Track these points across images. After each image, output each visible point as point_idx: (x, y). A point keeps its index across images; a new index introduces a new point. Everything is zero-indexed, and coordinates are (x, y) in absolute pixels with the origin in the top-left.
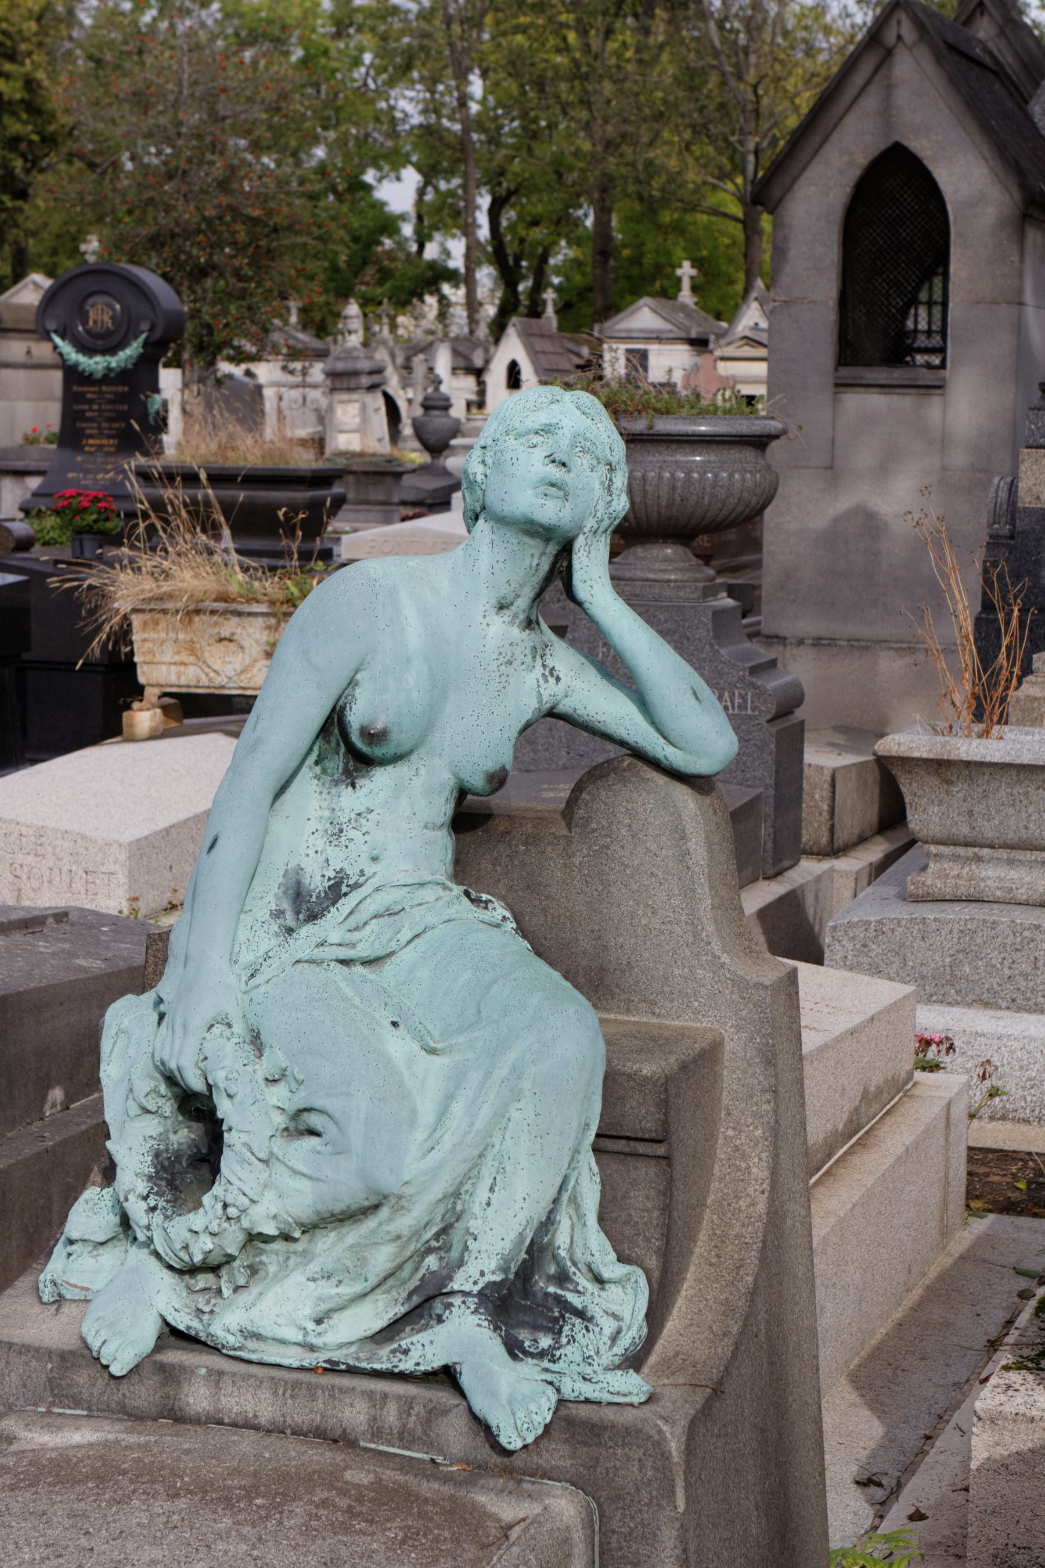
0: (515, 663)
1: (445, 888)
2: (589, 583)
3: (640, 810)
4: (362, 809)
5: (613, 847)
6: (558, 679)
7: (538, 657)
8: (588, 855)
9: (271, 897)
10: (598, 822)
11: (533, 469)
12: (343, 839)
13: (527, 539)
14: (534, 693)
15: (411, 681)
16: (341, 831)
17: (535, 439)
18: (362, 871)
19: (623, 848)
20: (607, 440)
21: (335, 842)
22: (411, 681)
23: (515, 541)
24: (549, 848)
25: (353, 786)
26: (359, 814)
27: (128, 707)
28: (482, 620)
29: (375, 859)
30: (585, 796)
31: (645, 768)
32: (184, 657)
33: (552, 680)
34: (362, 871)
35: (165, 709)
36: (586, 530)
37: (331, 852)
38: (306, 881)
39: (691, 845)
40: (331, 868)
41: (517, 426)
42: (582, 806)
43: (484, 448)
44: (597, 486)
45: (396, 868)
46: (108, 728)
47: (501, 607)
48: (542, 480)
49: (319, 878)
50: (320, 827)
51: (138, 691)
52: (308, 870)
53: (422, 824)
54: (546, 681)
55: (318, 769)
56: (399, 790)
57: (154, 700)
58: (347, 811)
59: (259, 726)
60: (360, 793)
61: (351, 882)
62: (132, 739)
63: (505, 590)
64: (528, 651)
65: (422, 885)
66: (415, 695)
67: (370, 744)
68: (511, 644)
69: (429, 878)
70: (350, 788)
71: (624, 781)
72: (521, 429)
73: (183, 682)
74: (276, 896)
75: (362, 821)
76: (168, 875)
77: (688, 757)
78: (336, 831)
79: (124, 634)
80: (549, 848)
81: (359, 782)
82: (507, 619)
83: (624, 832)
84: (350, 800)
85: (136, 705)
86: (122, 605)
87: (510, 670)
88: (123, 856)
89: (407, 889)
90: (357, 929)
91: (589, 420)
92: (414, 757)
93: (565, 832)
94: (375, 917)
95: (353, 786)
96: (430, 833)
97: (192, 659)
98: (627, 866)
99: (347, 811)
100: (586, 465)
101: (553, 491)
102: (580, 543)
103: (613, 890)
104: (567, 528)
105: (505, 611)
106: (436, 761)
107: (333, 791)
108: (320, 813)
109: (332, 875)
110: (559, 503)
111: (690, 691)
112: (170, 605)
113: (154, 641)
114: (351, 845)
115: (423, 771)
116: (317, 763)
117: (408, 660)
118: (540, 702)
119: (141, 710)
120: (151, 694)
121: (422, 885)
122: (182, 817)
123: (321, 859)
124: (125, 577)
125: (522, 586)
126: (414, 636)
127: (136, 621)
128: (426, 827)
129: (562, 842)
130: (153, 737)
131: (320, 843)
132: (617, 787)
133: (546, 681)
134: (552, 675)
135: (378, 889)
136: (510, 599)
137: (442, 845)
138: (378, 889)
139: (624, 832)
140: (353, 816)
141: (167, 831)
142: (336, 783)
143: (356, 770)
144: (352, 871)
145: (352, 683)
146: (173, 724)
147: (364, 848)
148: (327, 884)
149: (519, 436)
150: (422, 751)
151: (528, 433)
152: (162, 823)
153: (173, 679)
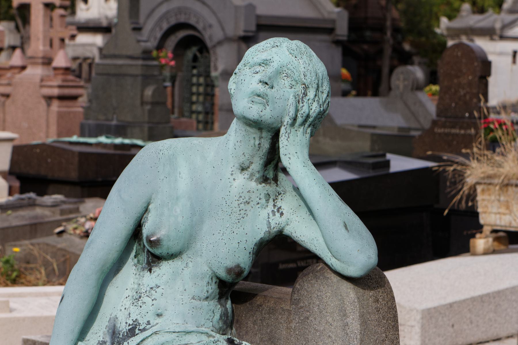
0: (252, 204)
1: (209, 336)
2: (288, 156)
3: (324, 296)
4: (153, 285)
5: (310, 319)
6: (282, 214)
7: (271, 200)
8: (299, 322)
9: (101, 334)
10: (304, 303)
11: (251, 86)
13: (248, 128)
14: (265, 222)
15: (178, 210)
16: (140, 297)
17: (258, 68)
19: (315, 319)
20: (303, 69)
21: (135, 304)
22: (178, 210)
23: (243, 129)
25: (150, 270)
26: (152, 288)
27: (473, 236)
28: (230, 176)
29: (159, 315)
32: (503, 210)
33: (278, 215)
35: (497, 239)
36: (285, 123)
37: (133, 309)
38: (118, 325)
39: (349, 320)
40: (131, 319)
41: (250, 61)
44: (291, 97)
45: (171, 322)
46: (462, 248)
47: (243, 169)
48: (252, 92)
49: (124, 324)
50: (131, 294)
51: (479, 228)
52: (120, 319)
53: (191, 297)
54: (274, 215)
55: (136, 260)
56: (175, 275)
57: (488, 233)
58: (146, 286)
60: (154, 275)
61: (141, 328)
62: (475, 254)
63: (242, 159)
64: (262, 196)
66: (180, 219)
67: (151, 247)
68: (249, 192)
69: (195, 329)
70: (149, 273)
71: (317, 278)
73: (503, 223)
74: (104, 334)
75: (153, 292)
76: (451, 329)
77: (343, 265)
78: (138, 297)
79: (472, 196)
80: (280, 317)
81: (154, 269)
82: (246, 176)
83: (316, 309)
84: (149, 279)
85: (478, 235)
86: (470, 180)
87: (248, 207)
88: (419, 317)
89: (176, 334)
91: (293, 58)
92: (184, 256)
95: (150, 270)
96: (197, 303)
97: (507, 212)
98: (317, 331)
99: (146, 286)
100: (287, 84)
101: (257, 99)
102: (282, 130)
104: (270, 121)
105: (245, 172)
106: (199, 259)
107: (141, 273)
108: (133, 286)
109: (131, 322)
110: (261, 107)
111: (342, 224)
112: (496, 181)
113: (489, 201)
114: (144, 306)
115: (190, 265)
116: (135, 257)
117: (177, 198)
118: (269, 227)
119: (480, 238)
120: (487, 230)
122: (463, 297)
123: (127, 313)
124: (474, 164)
125: (253, 156)
126: (183, 184)
127: (479, 189)
128: (193, 298)
130: (486, 253)
131: (128, 303)
132: (313, 282)
133: (274, 215)
134: (278, 211)
135: (156, 333)
136: (247, 164)
137: (213, 311)
138: (156, 333)
139: (316, 309)
140: (148, 289)
141: (451, 305)
142: (143, 269)
143: (153, 262)
144: (142, 322)
145: (146, 210)
146: (502, 247)
147: (151, 308)
148: (128, 328)
150: (190, 253)
151: (255, 65)
152: (450, 300)
153: (498, 222)
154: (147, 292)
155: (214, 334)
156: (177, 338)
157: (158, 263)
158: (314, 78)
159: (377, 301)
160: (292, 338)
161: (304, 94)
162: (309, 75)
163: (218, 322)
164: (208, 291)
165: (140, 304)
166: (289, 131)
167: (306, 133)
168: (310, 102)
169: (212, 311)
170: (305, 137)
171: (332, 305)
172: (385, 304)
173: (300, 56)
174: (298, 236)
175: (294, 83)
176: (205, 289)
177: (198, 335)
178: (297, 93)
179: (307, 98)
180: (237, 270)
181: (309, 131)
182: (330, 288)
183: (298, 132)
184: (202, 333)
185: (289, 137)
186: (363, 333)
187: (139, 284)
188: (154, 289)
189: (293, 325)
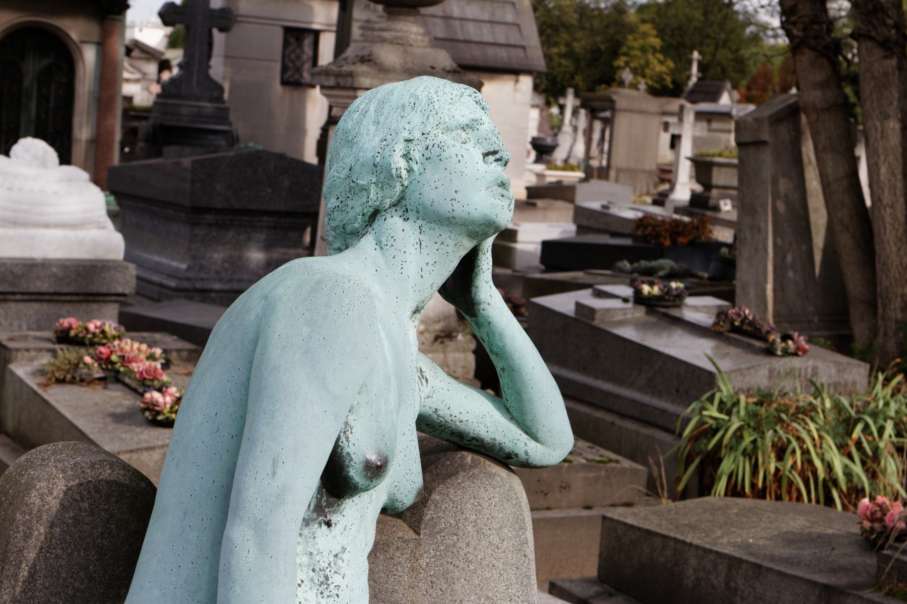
3: (485, 505)
4: (337, 549)
12: (332, 587)
16: (327, 578)
19: (468, 545)
21: (326, 593)
23: (451, 242)
24: (398, 554)
26: (336, 556)
30: (435, 497)
31: (488, 463)
41: (447, 120)
42: (432, 507)
43: (408, 141)
59: (280, 472)
60: (336, 530)
70: (324, 527)
72: (452, 123)
78: (322, 579)
83: (469, 528)
93: (414, 536)
95: (329, 524)
98: (471, 562)
103: (457, 587)
107: (306, 532)
114: (340, 593)
129: (411, 545)
139: (469, 528)
140: (332, 558)
143: (329, 505)
149: (448, 130)
154: (332, 565)
157: (339, 505)
160: (421, 584)
165: (335, 592)
171: (501, 515)
174: (456, 413)
182: (498, 489)
187: (311, 554)
188: (340, 556)
189: (423, 562)
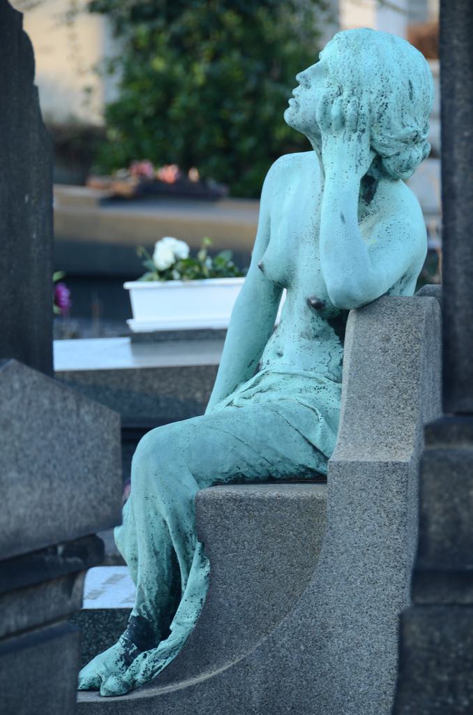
18: (268, 361)
29: (280, 355)
34: (268, 361)
65: (293, 375)
69: (301, 371)
89: (282, 376)
90: (250, 398)
91: (338, 52)
94: (261, 391)
96: (305, 341)
121: (293, 375)
155: (325, 380)
156: (283, 381)
158: (346, 76)
159: (388, 340)
161: (337, 93)
162: (341, 70)
163: (338, 368)
164: (314, 329)
166: (326, 138)
167: (349, 141)
168: (344, 102)
169: (327, 353)
170: (346, 145)
172: (400, 346)
173: (344, 49)
175: (331, 81)
176: (311, 325)
177: (304, 379)
178: (331, 93)
179: (340, 98)
180: (313, 302)
181: (355, 136)
183: (337, 139)
184: (310, 378)
185: (326, 145)
186: (353, 374)
